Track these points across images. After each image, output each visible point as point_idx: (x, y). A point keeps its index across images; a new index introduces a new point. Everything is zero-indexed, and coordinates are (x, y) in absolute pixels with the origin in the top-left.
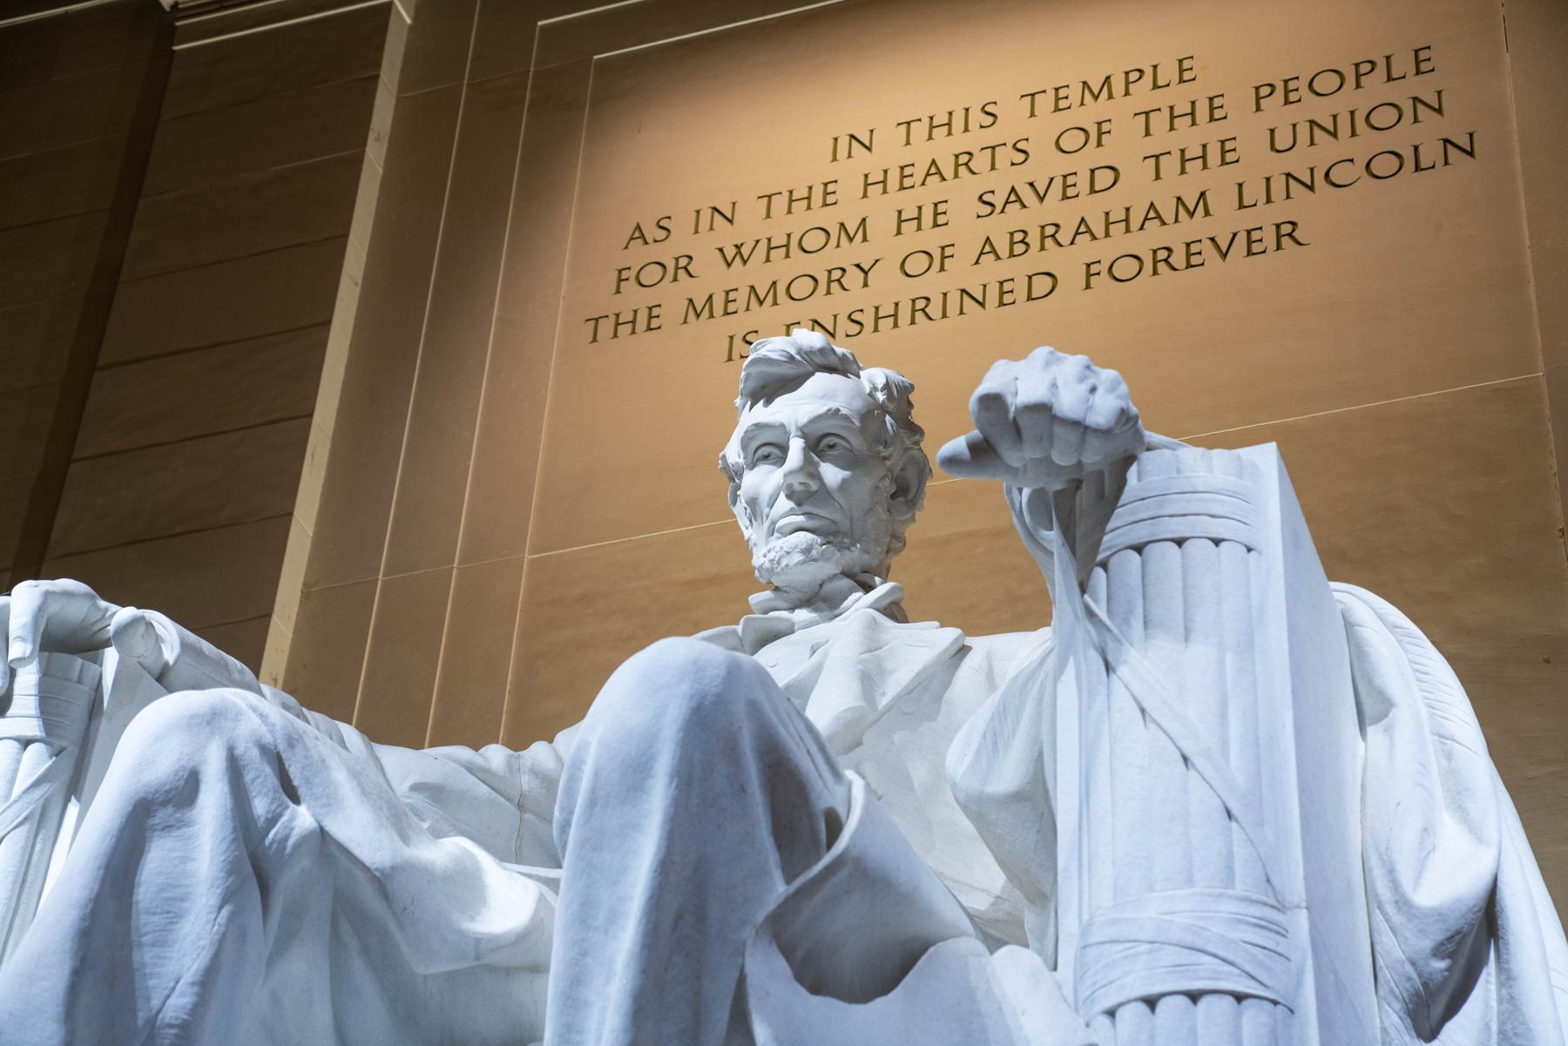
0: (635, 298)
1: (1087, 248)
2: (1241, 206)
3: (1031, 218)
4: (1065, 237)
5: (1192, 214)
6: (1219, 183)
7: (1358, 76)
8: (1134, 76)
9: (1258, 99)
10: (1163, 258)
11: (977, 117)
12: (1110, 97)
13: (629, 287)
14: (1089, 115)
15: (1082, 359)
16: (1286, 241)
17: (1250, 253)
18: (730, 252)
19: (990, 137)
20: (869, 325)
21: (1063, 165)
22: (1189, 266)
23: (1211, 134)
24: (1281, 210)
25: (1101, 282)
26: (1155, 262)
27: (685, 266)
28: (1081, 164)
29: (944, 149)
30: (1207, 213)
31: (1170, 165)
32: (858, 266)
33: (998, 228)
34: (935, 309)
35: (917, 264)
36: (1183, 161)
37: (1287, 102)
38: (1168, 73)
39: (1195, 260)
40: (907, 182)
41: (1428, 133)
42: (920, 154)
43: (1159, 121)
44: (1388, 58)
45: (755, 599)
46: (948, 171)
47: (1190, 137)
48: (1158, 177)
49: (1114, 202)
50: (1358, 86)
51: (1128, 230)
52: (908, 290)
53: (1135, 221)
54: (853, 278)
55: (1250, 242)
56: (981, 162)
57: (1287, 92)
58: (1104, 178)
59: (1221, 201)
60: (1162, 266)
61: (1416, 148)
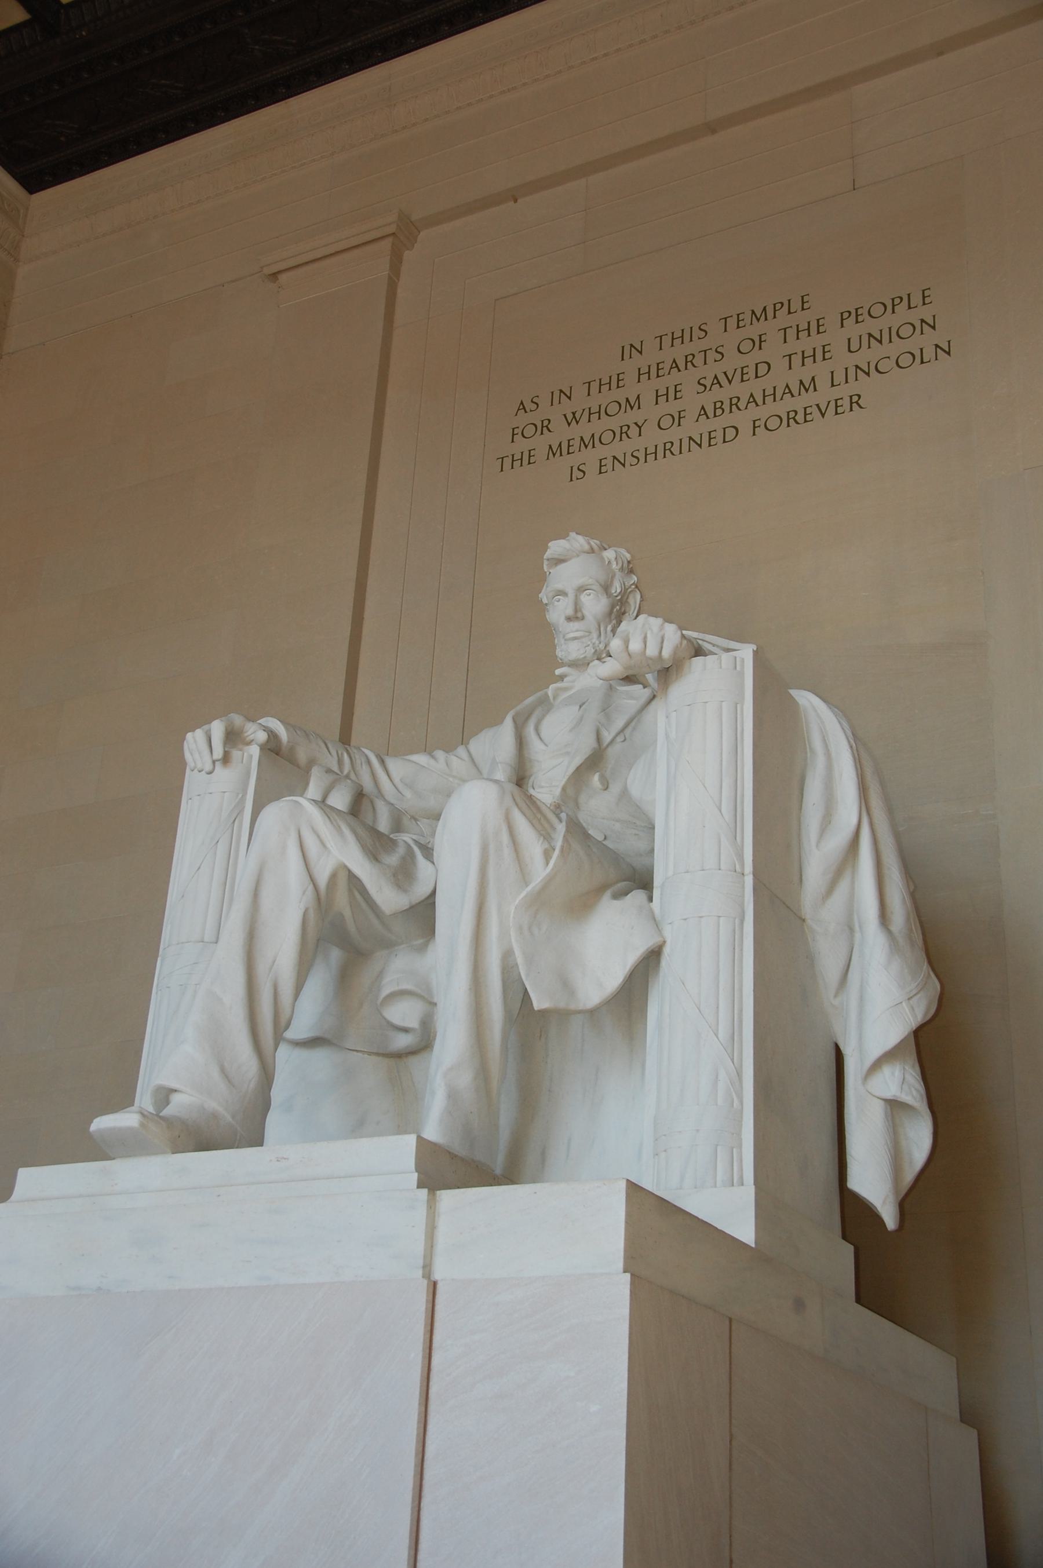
0: (522, 445)
1: (754, 412)
2: (833, 385)
3: (724, 394)
4: (742, 405)
5: (807, 390)
6: (821, 370)
7: (894, 306)
9: (842, 320)
10: (791, 418)
11: (697, 333)
13: (518, 438)
14: (754, 330)
15: (660, 621)
16: (854, 405)
17: (836, 413)
18: (570, 417)
19: (704, 344)
20: (642, 460)
21: (740, 361)
22: (806, 421)
23: (817, 341)
24: (853, 388)
26: (788, 419)
27: (545, 427)
28: (750, 360)
29: (679, 352)
30: (815, 390)
31: (797, 360)
32: (636, 424)
33: (708, 399)
34: (676, 449)
35: (666, 422)
36: (803, 358)
37: (857, 322)
38: (796, 305)
40: (661, 373)
41: (927, 340)
42: (668, 355)
43: (791, 333)
45: (558, 672)
46: (682, 366)
47: (807, 344)
48: (790, 368)
49: (766, 383)
50: (893, 312)
52: (661, 438)
53: (778, 398)
54: (634, 431)
55: (837, 407)
56: (699, 360)
57: (857, 316)
60: (791, 421)
61: (922, 350)
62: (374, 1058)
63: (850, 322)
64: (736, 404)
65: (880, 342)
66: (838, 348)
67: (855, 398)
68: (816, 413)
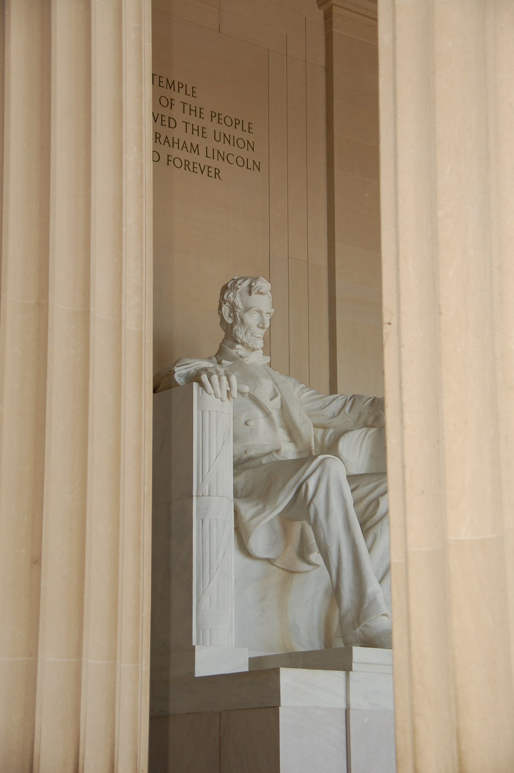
4: (162, 140)
6: (203, 143)
7: (236, 124)
8: (181, 86)
9: (212, 116)
10: (186, 164)
12: (174, 90)
25: (171, 163)
26: (185, 165)
30: (198, 154)
36: (193, 129)
38: (190, 91)
39: (195, 170)
43: (187, 108)
44: (243, 121)
45: (238, 346)
48: (186, 132)
51: (178, 148)
53: (180, 148)
57: (219, 119)
58: (173, 124)
59: (202, 151)
62: (281, 570)
63: (215, 119)
64: (159, 138)
65: (229, 142)
66: (210, 134)
67: (217, 172)
68: (198, 170)
